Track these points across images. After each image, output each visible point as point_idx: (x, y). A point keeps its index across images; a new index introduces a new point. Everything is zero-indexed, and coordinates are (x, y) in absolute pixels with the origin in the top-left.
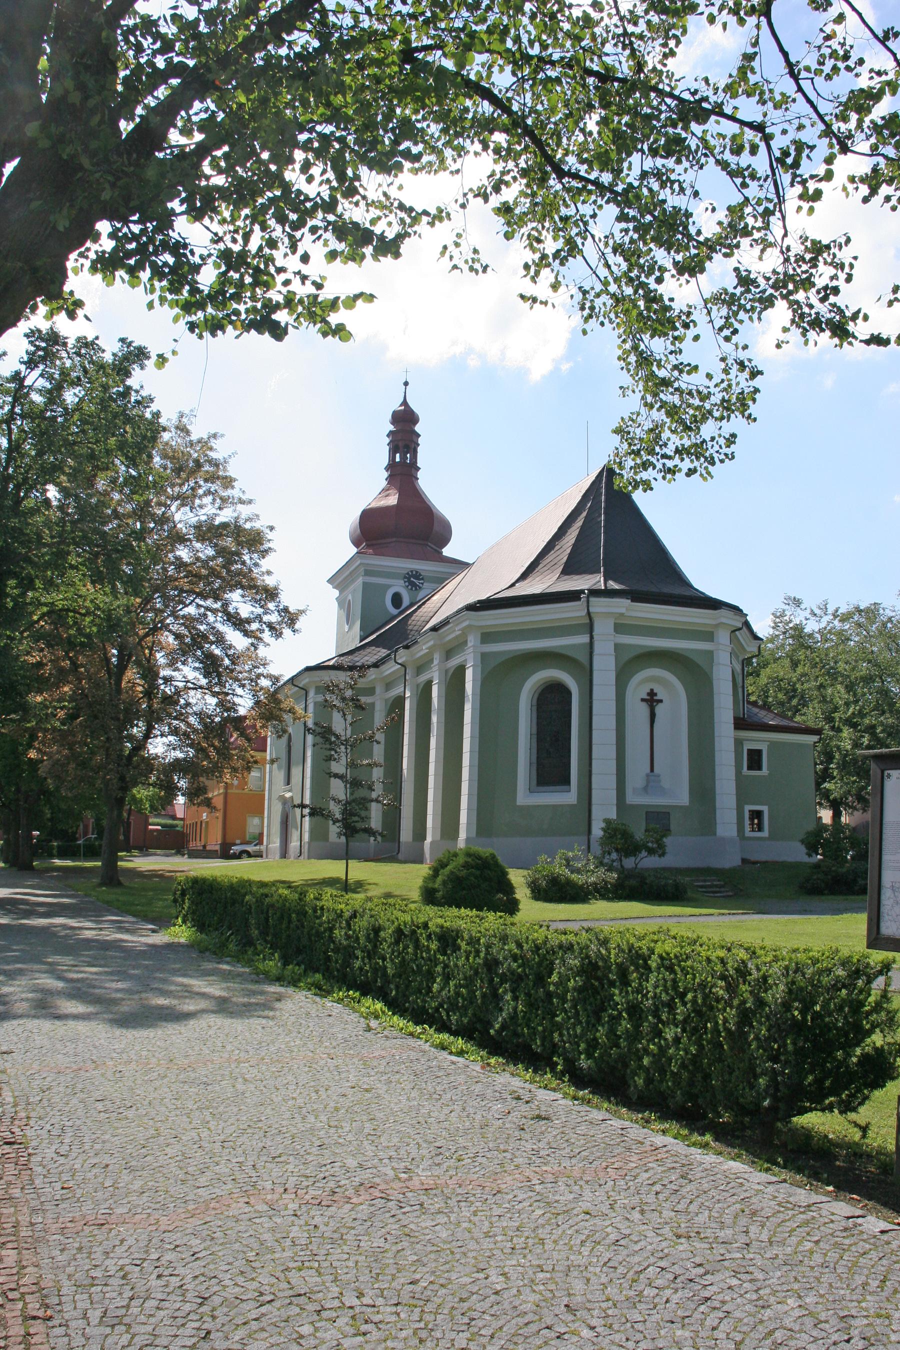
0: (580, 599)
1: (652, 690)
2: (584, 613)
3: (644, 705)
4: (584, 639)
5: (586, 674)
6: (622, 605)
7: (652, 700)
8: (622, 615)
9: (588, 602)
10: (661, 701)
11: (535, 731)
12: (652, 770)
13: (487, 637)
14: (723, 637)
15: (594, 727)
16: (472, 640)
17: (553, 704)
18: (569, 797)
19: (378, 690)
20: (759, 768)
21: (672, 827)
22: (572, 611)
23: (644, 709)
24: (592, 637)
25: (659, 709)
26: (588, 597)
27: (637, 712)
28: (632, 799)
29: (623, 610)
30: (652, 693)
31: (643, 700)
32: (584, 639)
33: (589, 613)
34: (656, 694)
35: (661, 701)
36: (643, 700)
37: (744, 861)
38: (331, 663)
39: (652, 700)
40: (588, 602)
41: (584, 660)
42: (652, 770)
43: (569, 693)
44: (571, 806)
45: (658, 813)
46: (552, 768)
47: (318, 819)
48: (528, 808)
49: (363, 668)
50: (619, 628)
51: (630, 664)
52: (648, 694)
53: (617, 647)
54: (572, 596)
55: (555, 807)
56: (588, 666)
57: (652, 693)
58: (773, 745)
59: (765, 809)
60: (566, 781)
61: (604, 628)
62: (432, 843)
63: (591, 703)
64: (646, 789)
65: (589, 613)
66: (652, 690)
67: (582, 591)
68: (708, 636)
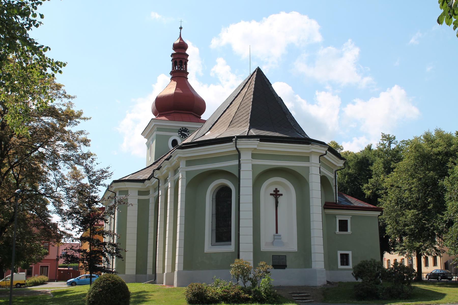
0: (232, 141)
1: (276, 189)
2: (235, 149)
3: (272, 197)
4: (236, 162)
5: (237, 180)
6: (255, 144)
7: (276, 194)
8: (255, 149)
9: (236, 142)
10: (281, 195)
11: (214, 212)
12: (277, 232)
13: (190, 162)
14: (315, 160)
15: (241, 210)
16: (182, 164)
17: (224, 198)
18: (231, 248)
19: (151, 192)
20: (347, 230)
21: (288, 264)
22: (228, 148)
23: (272, 200)
24: (239, 161)
25: (280, 199)
26: (236, 140)
27: (267, 201)
28: (264, 248)
29: (256, 147)
30: (276, 191)
31: (271, 194)
32: (236, 162)
33: (237, 149)
34: (278, 191)
35: (281, 195)
36: (271, 194)
37: (328, 282)
38: (127, 178)
39: (276, 194)
40: (236, 142)
41: (236, 174)
42: (277, 232)
43: (230, 190)
44: (232, 253)
45: (279, 256)
46: (223, 233)
47: (120, 259)
48: (211, 254)
49: (143, 181)
50: (254, 156)
51: (261, 177)
52: (274, 191)
53: (253, 165)
54: (228, 140)
55: (223, 253)
56: (238, 177)
57: (276, 191)
58: (353, 217)
59: (350, 253)
60: (229, 239)
61: (246, 157)
62: (178, 272)
63: (239, 197)
64: (273, 243)
65: (237, 149)
66: (276, 189)
67: (234, 137)
68: (306, 158)
